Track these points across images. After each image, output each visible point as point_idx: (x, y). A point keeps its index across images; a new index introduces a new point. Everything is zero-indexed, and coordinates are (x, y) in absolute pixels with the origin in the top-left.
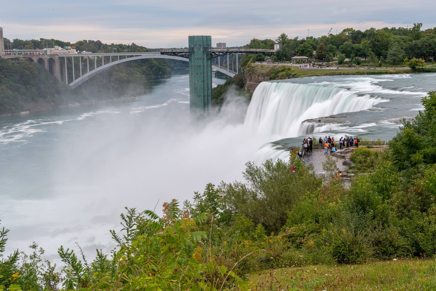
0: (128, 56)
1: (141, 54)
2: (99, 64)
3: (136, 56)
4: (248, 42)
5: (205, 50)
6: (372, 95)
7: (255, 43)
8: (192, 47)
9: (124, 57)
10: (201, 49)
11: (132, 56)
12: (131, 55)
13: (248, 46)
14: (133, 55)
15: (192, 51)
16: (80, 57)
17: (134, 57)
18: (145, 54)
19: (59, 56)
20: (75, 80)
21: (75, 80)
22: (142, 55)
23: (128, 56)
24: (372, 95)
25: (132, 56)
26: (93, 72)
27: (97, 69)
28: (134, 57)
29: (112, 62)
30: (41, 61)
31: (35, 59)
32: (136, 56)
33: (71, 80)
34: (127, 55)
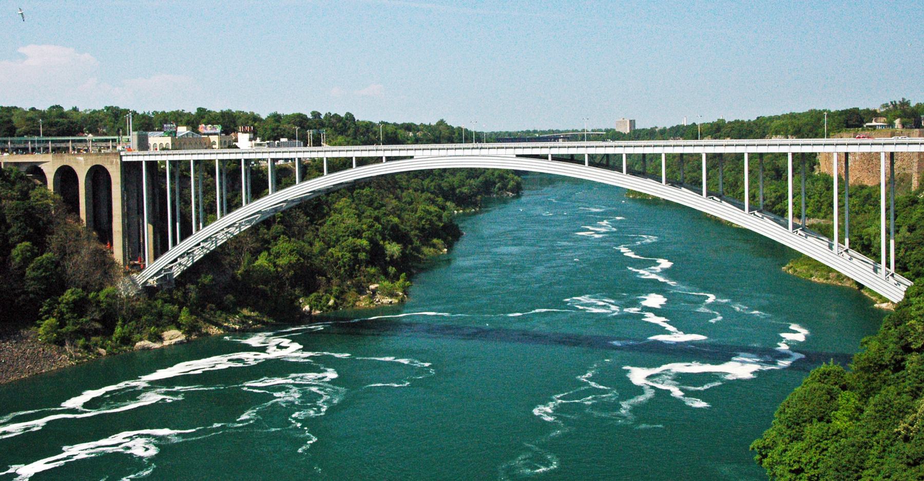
0: (362, 162)
1: (410, 153)
2: (258, 190)
3: (389, 159)
11: (379, 160)
14: (379, 154)
16: (217, 161)
17: (382, 161)
18: (427, 153)
19: (125, 159)
22: (412, 157)
23: (362, 162)
25: (379, 160)
26: (237, 215)
27: (273, 200)
28: (382, 161)
30: (66, 175)
32: (389, 159)
34: (359, 154)
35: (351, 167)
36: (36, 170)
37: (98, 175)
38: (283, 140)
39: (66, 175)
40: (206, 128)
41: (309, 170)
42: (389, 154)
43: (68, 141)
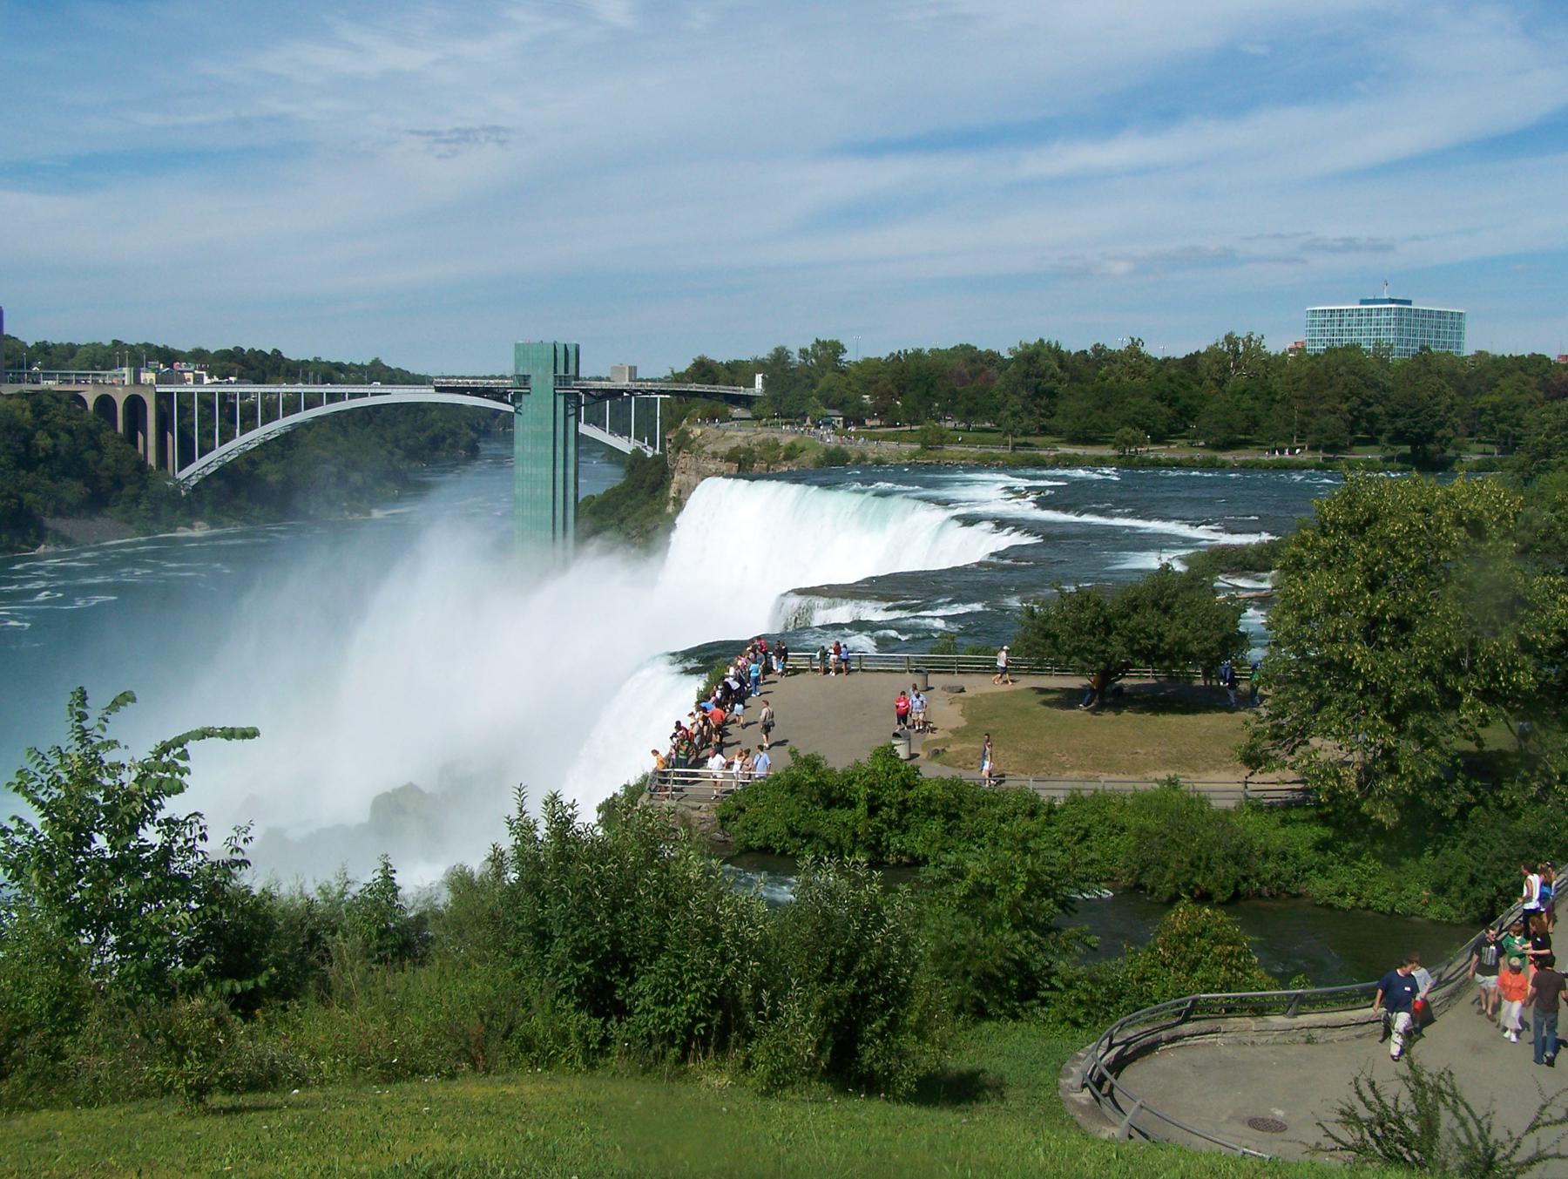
0: (353, 396)
1: (388, 391)
2: (270, 416)
3: (373, 394)
4: (683, 366)
5: (561, 385)
6: (1001, 523)
7: (704, 370)
8: (526, 373)
9: (340, 397)
10: (551, 380)
11: (365, 395)
12: (361, 391)
13: (678, 378)
15: (525, 384)
19: (158, 390)
20: (199, 457)
21: (200, 457)
23: (353, 396)
24: (1001, 523)
25: (365, 395)
29: (305, 409)
30: (105, 403)
31: (90, 396)
32: (373, 394)
33: (186, 459)
35: (344, 399)
36: (77, 398)
37: (135, 405)
38: (232, 379)
39: (105, 403)
40: (180, 366)
41: (313, 401)
42: (373, 391)
43: (88, 374)
